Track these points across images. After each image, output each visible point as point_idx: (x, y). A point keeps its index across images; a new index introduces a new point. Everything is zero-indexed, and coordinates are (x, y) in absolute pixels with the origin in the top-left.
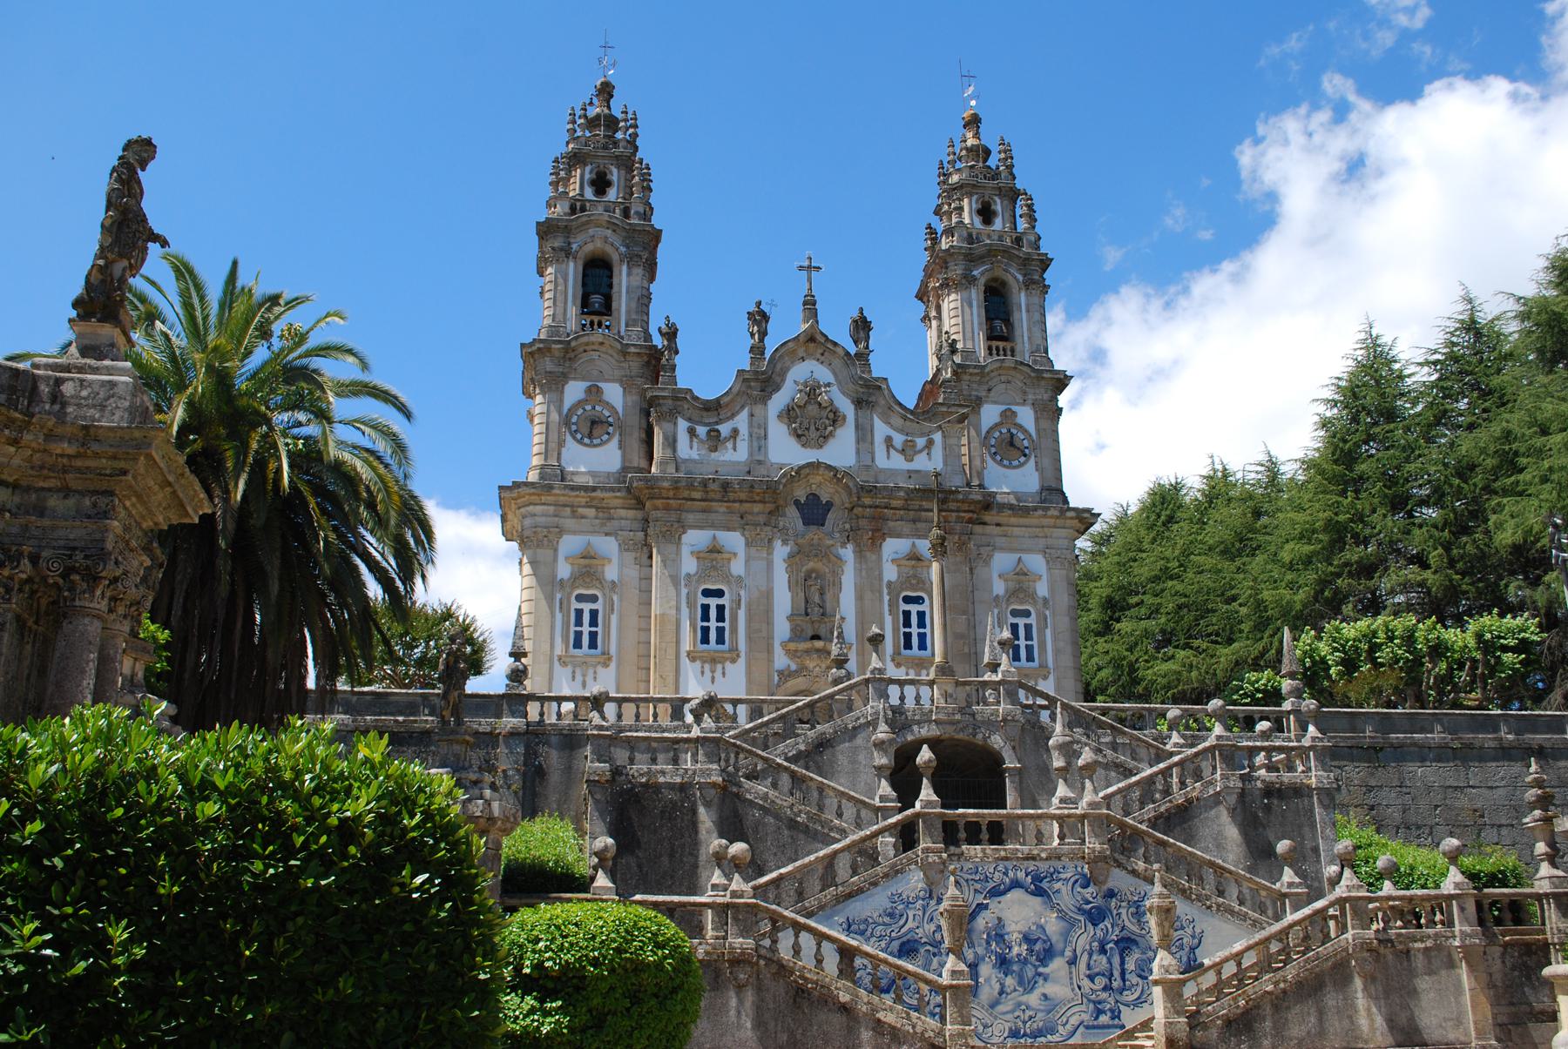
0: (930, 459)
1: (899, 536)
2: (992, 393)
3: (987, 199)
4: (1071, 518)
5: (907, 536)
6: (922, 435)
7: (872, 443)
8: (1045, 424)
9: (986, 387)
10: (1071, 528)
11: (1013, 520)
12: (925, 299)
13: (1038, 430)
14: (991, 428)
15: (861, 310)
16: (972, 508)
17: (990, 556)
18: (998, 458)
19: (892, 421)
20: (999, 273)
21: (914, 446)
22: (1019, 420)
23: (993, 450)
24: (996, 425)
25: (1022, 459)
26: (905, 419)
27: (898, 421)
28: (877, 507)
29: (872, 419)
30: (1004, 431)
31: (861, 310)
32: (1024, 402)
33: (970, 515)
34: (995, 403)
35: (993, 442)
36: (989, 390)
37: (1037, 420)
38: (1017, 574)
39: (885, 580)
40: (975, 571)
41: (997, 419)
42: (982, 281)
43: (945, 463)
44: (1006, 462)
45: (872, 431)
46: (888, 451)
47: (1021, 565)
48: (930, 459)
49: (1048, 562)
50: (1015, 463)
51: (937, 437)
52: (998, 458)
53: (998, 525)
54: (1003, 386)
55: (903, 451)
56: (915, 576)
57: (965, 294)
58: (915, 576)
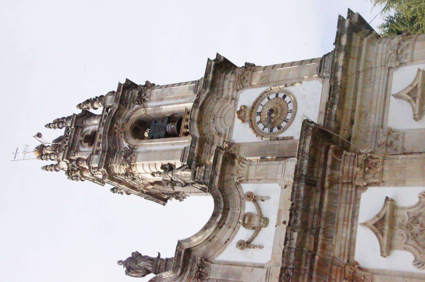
0: (268, 198)
1: (352, 243)
2: (222, 131)
3: (82, 138)
4: (350, 40)
5: (353, 232)
6: (242, 205)
7: (243, 265)
8: (256, 78)
9: (216, 137)
10: (362, 39)
11: (348, 105)
12: (166, 197)
13: (261, 85)
14: (255, 132)
15: (120, 262)
16: (323, 149)
17: (390, 132)
18: (284, 124)
19: (225, 239)
20: (128, 127)
21: (250, 216)
22: (249, 104)
23: (275, 130)
24: (252, 127)
25: (287, 99)
26: (220, 226)
27: (225, 233)
28: (311, 268)
29: (220, 263)
30: (258, 119)
31: (120, 262)
32: (234, 99)
33: (331, 152)
34: (231, 128)
35: (267, 130)
36: (219, 134)
37: (251, 86)
38: (414, 99)
39: (415, 270)
40: (408, 150)
41: (247, 125)
42: (133, 141)
43: (274, 180)
44: (289, 116)
45: (231, 264)
46: (254, 247)
47: (404, 94)
48: (268, 198)
49: (401, 64)
50: (291, 106)
51: (247, 188)
52: (284, 124)
53: (352, 122)
54: (218, 120)
55: (257, 230)
56: (408, 227)
57: (140, 156)
58: (408, 227)
